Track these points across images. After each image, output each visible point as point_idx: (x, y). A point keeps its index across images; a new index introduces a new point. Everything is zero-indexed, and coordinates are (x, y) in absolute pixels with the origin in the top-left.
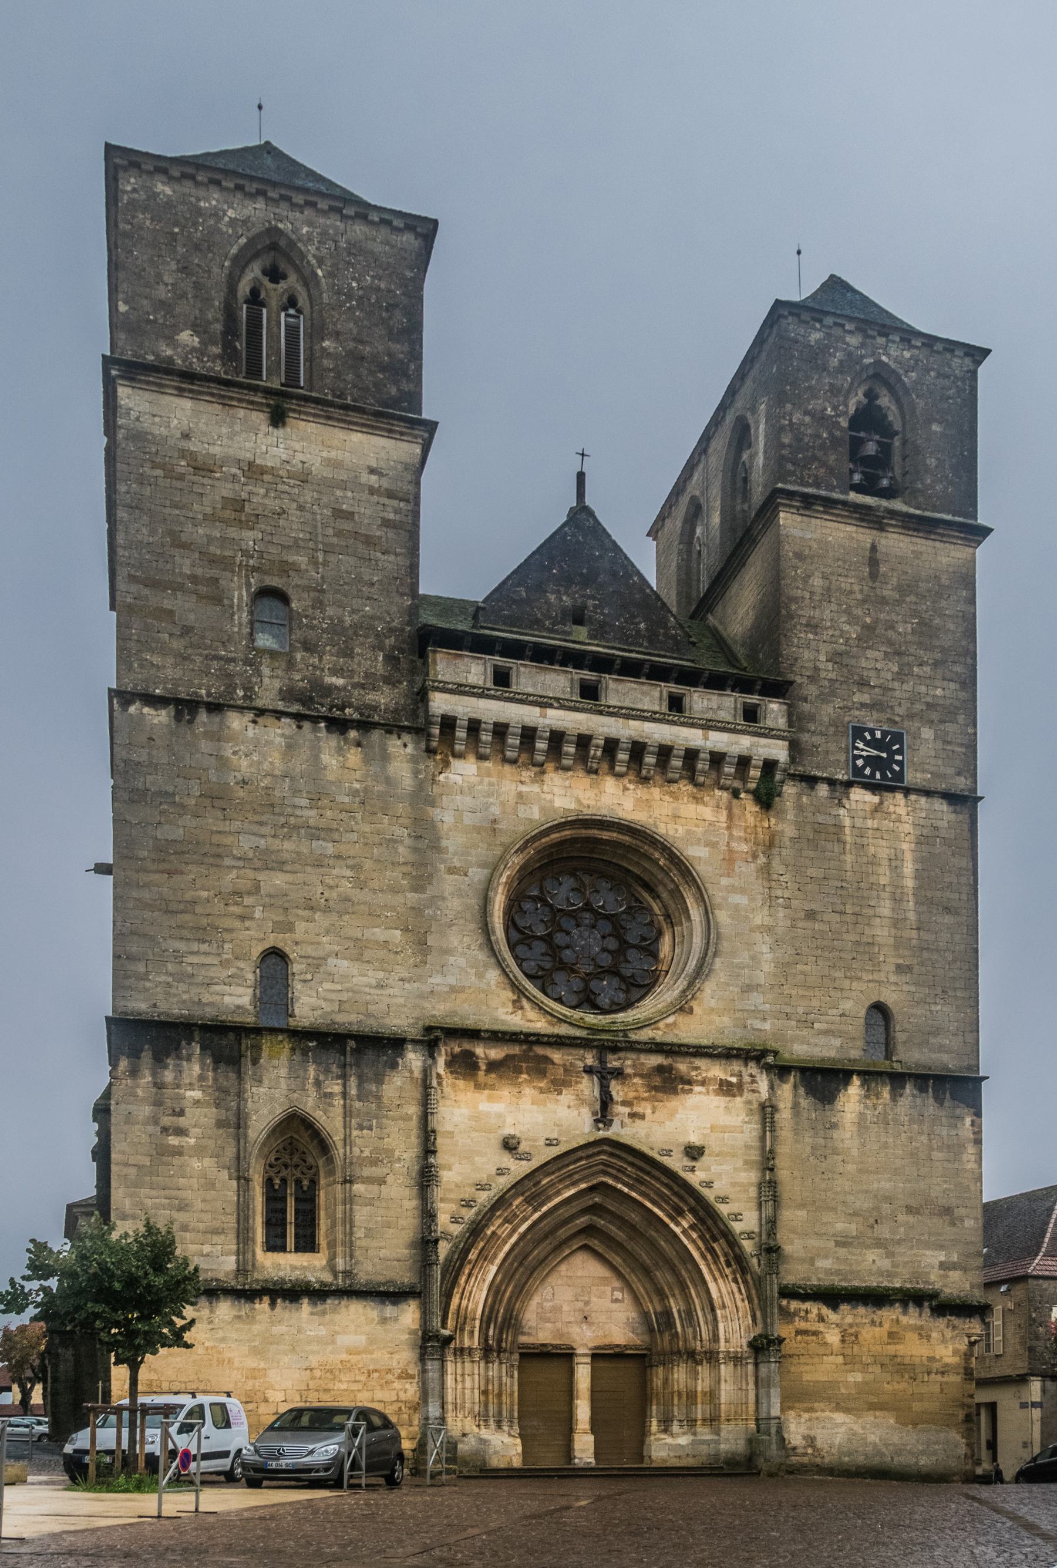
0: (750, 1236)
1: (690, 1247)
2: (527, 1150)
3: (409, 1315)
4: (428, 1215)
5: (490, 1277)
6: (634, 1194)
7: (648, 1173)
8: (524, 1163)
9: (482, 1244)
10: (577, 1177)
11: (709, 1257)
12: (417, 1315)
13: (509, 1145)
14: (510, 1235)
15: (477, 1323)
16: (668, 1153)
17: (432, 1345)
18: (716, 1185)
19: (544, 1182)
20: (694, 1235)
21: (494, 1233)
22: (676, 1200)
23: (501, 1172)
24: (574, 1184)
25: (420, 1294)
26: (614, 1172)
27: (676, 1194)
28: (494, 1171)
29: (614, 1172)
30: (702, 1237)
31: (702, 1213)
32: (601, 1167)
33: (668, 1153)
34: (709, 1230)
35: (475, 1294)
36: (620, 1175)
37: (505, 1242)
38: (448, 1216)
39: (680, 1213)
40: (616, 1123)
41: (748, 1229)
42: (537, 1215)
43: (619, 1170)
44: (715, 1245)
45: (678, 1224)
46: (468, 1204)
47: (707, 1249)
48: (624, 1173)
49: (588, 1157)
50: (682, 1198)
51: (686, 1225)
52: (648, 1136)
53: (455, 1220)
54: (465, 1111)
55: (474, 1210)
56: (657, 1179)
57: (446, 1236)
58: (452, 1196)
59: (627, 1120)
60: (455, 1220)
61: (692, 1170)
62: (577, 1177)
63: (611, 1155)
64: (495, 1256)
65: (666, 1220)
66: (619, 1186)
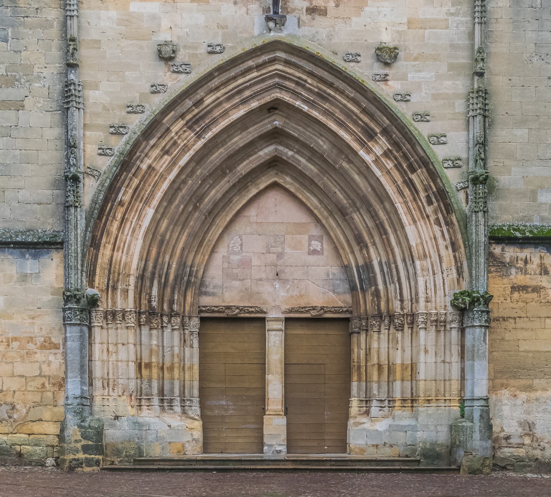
0: (455, 163)
1: (384, 180)
2: (186, 60)
3: (50, 271)
4: (70, 146)
5: (146, 222)
6: (315, 114)
7: (331, 85)
8: (182, 77)
9: (136, 181)
10: (247, 93)
11: (407, 192)
12: (61, 271)
13: (166, 56)
14: (169, 169)
15: (132, 280)
16: (354, 58)
17: (79, 308)
18: (414, 99)
19: (208, 100)
20: (390, 165)
21: (150, 167)
22: (366, 119)
23: (156, 90)
24: (244, 102)
25: (62, 243)
26: (292, 85)
27: (364, 111)
28: (147, 88)
29: (292, 85)
30: (398, 166)
31: (396, 135)
32: (277, 80)
33: (354, 58)
34: (405, 156)
35: (129, 245)
36: (299, 90)
37: (163, 177)
38: (96, 147)
39: (371, 135)
40: (291, 20)
41: (453, 155)
42: (200, 144)
43: (297, 83)
44: (413, 177)
45: (369, 151)
46: (117, 131)
47: (405, 182)
48: (303, 86)
49: (259, 67)
50: (371, 116)
51: (379, 151)
52: (330, 37)
53: (103, 152)
54: (113, 13)
55: (125, 138)
56: (342, 93)
57: (92, 172)
58: (100, 121)
59: (305, 17)
60: (103, 152)
61: (385, 79)
62: (247, 93)
63: (287, 63)
64: (152, 194)
65: (355, 145)
66: (298, 103)
